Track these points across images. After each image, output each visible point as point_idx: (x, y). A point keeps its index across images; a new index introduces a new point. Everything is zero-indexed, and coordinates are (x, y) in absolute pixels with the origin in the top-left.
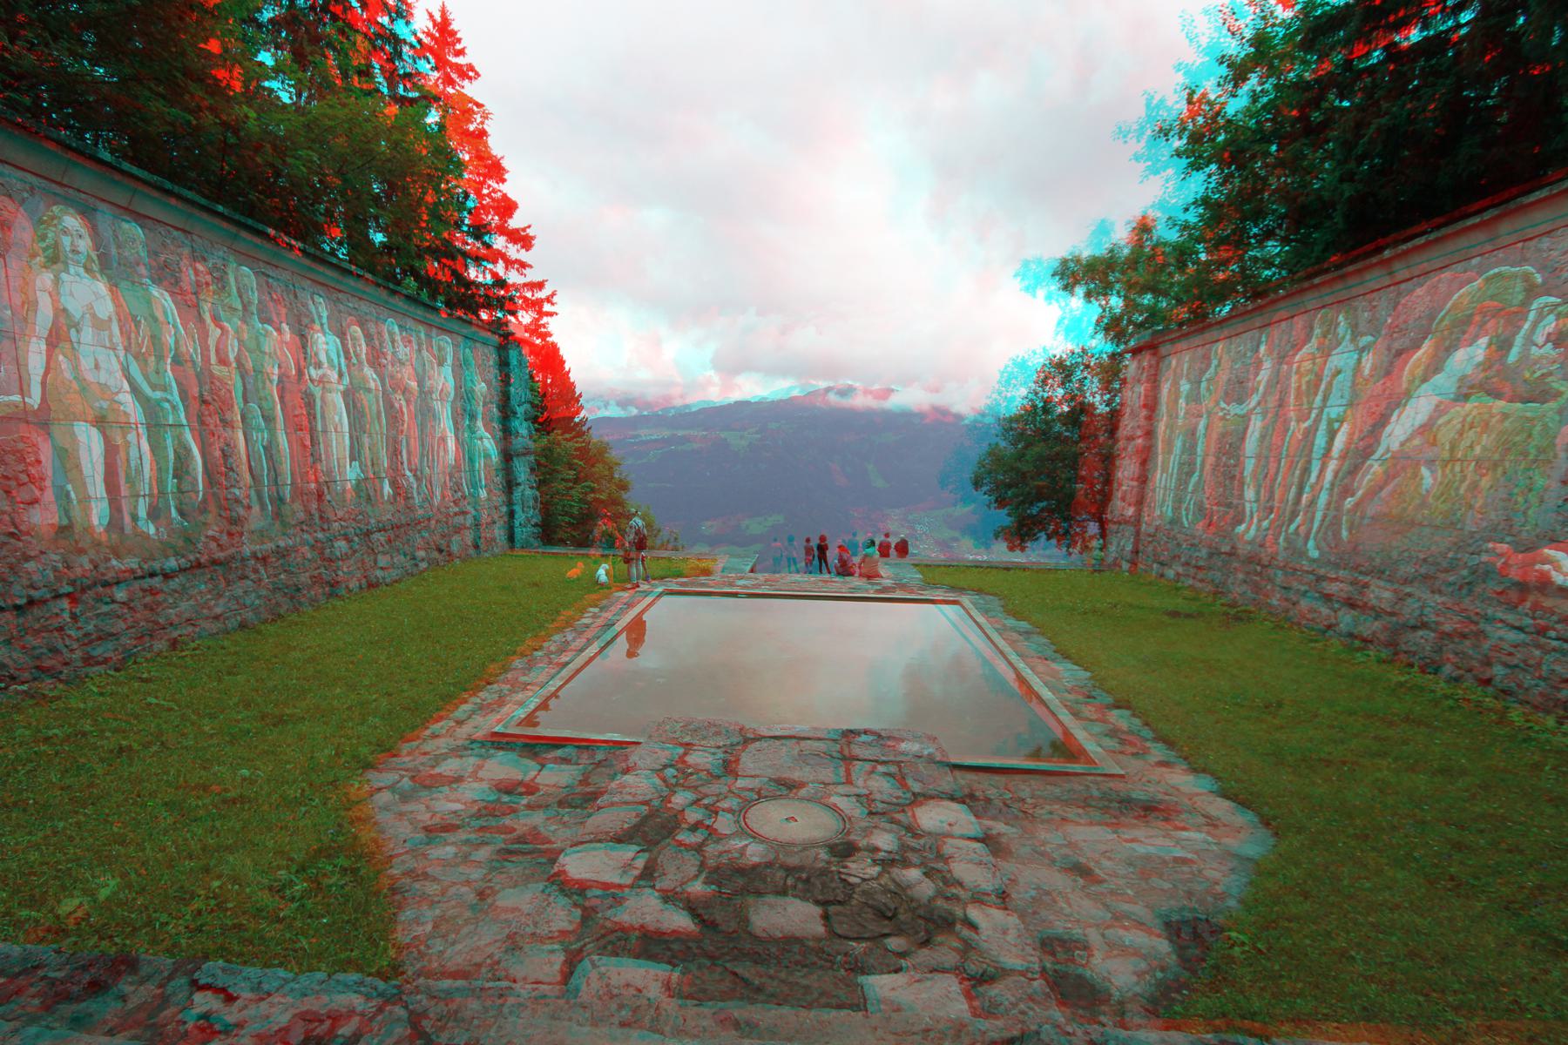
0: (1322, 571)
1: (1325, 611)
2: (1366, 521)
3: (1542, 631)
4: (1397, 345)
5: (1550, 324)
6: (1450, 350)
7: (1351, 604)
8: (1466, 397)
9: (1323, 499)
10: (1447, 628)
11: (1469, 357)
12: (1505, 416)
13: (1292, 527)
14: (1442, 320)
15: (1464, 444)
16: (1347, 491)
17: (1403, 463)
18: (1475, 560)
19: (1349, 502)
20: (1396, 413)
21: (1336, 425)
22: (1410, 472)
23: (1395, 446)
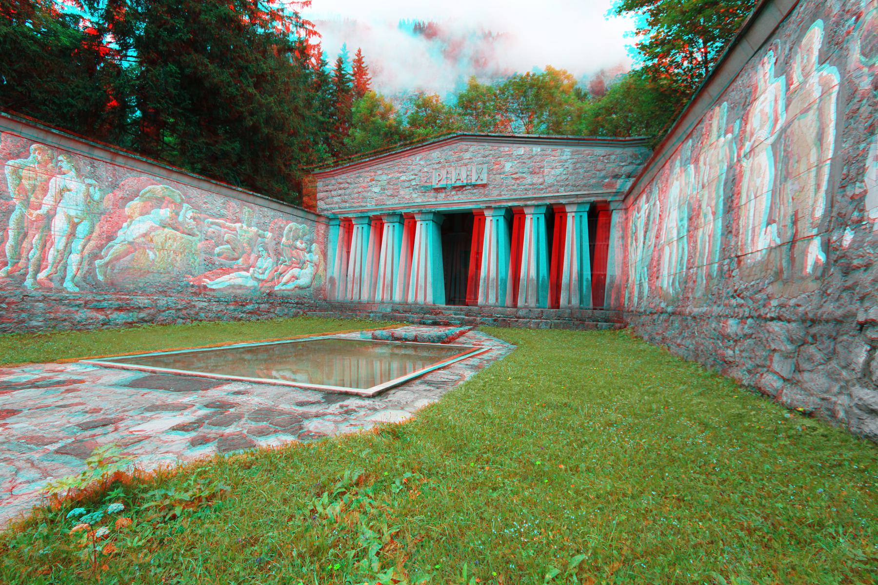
0: (89, 297)
1: (101, 317)
2: (115, 271)
3: (209, 301)
4: (119, 194)
5: (190, 214)
6: (152, 207)
7: (120, 309)
8: (164, 227)
9: (74, 258)
10: (180, 307)
11: (165, 213)
12: (182, 238)
13: (41, 276)
14: (146, 193)
15: (168, 244)
16: (96, 256)
17: (133, 246)
18: (183, 284)
19: (97, 262)
20: (125, 225)
21: (76, 220)
22: (141, 251)
23: (131, 240)
